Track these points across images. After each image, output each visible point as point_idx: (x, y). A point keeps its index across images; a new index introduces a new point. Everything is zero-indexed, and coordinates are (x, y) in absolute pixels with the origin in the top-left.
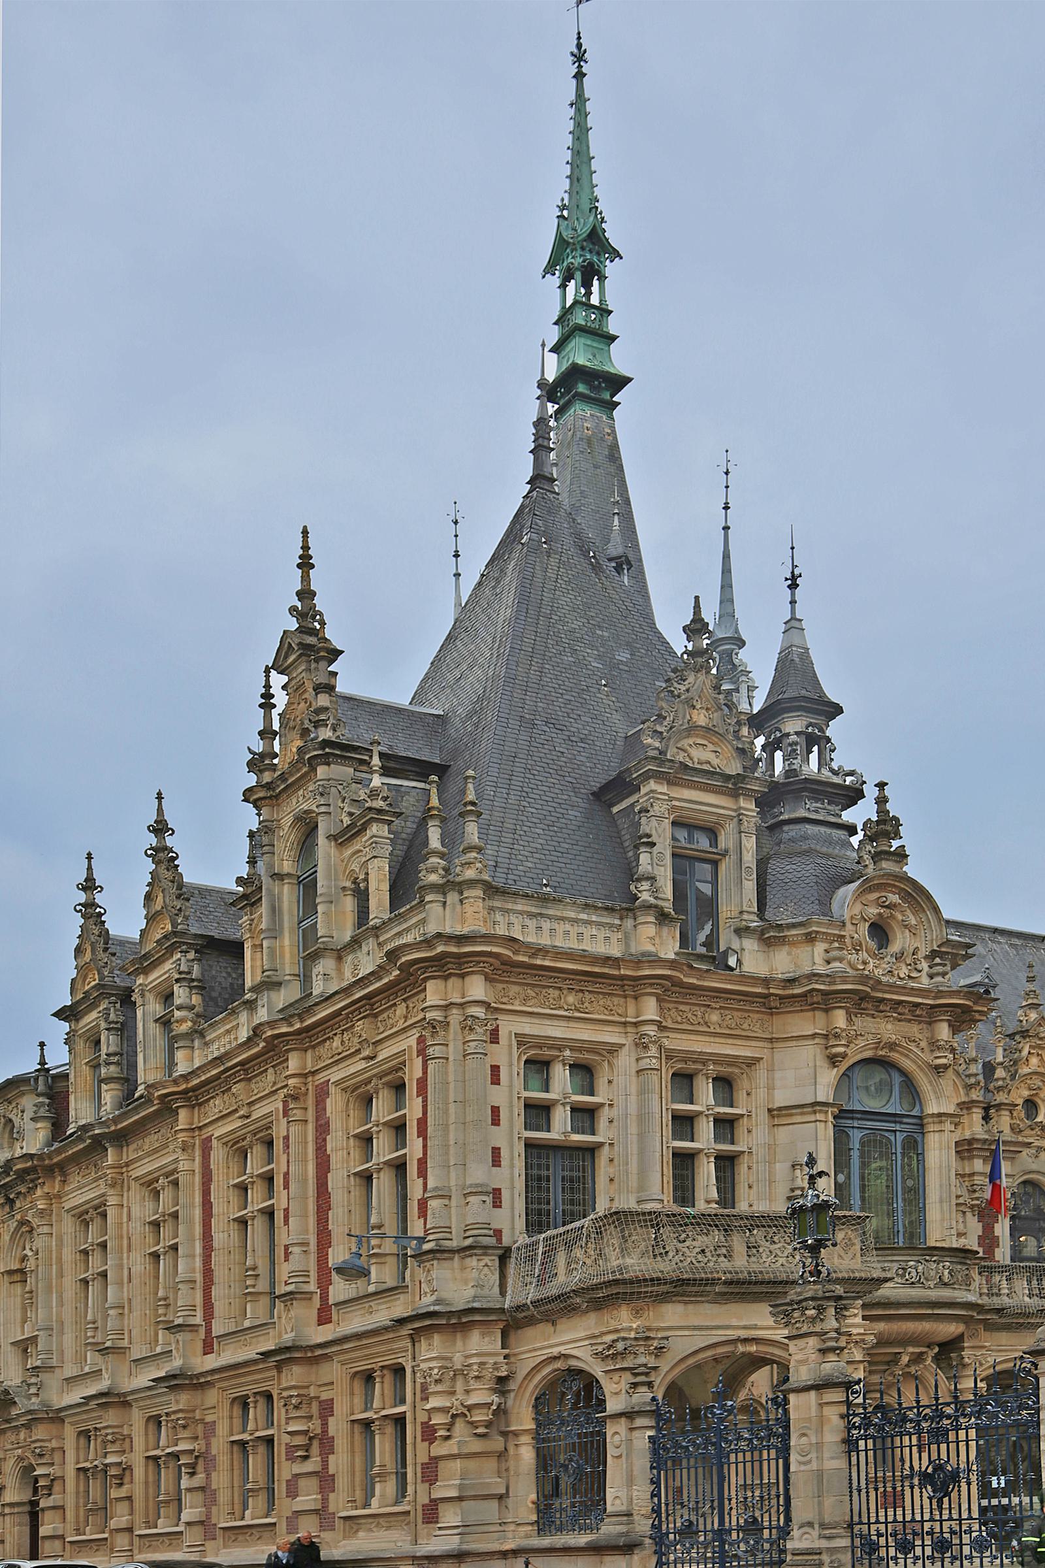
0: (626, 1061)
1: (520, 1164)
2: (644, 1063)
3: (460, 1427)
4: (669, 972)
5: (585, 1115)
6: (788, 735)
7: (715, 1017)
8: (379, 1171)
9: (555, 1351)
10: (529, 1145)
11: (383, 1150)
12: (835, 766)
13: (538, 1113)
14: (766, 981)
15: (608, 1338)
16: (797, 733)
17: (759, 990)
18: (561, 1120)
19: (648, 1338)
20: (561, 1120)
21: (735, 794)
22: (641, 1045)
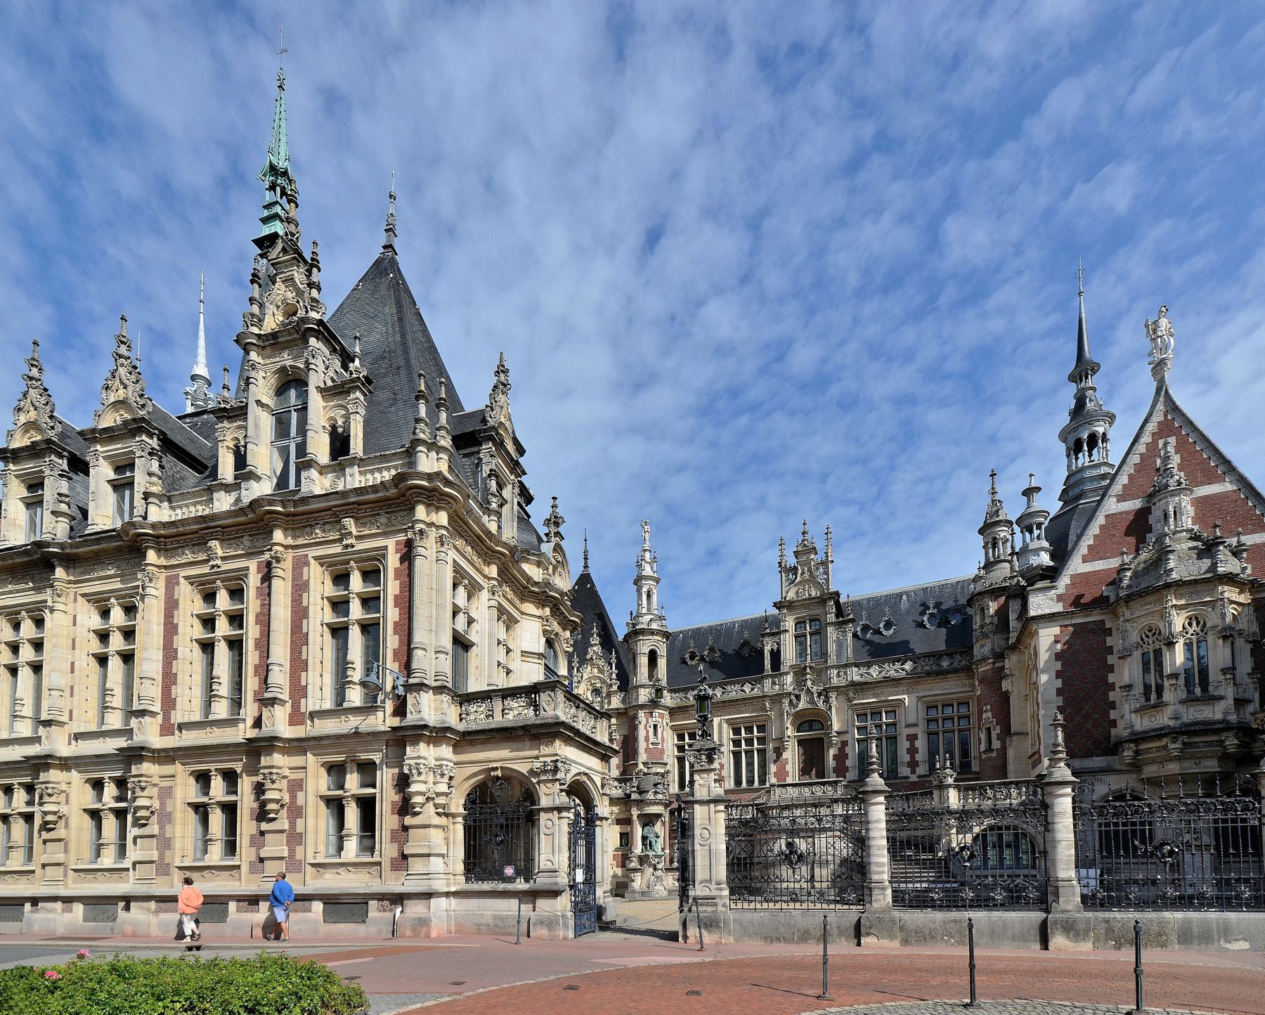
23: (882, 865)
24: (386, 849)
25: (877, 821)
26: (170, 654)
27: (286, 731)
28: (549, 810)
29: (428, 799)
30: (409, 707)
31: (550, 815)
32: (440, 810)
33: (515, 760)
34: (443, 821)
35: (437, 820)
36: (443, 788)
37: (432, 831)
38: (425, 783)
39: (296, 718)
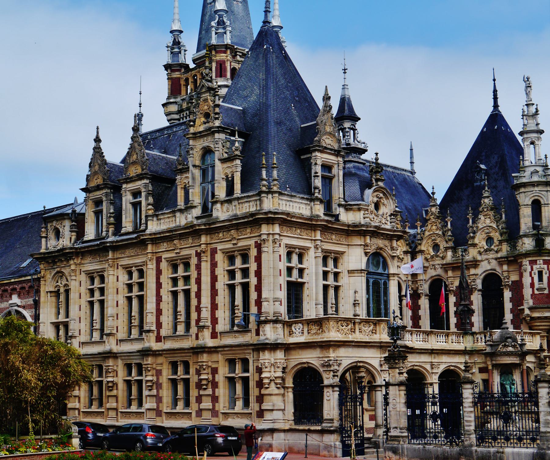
0: (312, 252)
1: (286, 290)
2: (317, 255)
3: (273, 384)
4: (325, 223)
5: (301, 271)
6: (345, 128)
7: (334, 237)
8: (238, 285)
9: (304, 361)
10: (289, 283)
11: (239, 278)
12: (359, 140)
13: (290, 270)
14: (349, 226)
15: (326, 360)
16: (349, 128)
17: (346, 228)
18: (295, 273)
19: (337, 360)
20: (295, 273)
21: (337, 156)
22: (316, 247)
23: (470, 421)
24: (254, 406)
25: (467, 398)
26: (159, 299)
27: (210, 343)
28: (328, 386)
29: (271, 380)
30: (261, 333)
31: (328, 390)
32: (279, 386)
33: (312, 358)
34: (282, 391)
35: (276, 391)
36: (279, 374)
37: (274, 398)
38: (270, 372)
39: (214, 335)
